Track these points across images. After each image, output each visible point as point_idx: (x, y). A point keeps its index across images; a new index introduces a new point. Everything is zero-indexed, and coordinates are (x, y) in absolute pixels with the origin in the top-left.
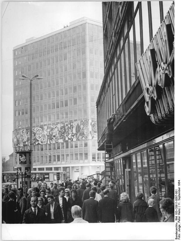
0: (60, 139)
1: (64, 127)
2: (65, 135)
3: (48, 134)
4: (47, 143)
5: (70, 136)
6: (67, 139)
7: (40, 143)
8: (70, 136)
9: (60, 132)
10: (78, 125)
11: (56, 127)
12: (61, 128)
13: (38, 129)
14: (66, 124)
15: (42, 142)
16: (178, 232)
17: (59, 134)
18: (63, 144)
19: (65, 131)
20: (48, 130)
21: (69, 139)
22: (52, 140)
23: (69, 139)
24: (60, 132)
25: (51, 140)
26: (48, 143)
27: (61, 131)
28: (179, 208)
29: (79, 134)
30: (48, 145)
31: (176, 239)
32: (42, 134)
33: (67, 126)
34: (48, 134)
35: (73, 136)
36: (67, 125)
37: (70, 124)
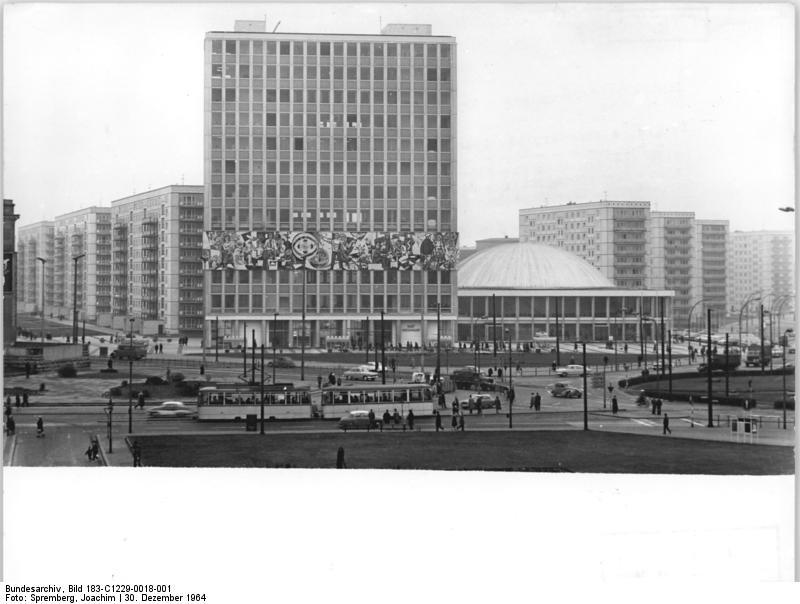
0: (373, 262)
2: (391, 256)
3: (336, 249)
4: (332, 268)
5: (403, 260)
6: (394, 264)
7: (308, 265)
8: (403, 260)
13: (301, 236)
14: (392, 234)
16: (27, 595)
17: (370, 252)
18: (378, 274)
19: (389, 246)
20: (337, 242)
21: (400, 264)
22: (348, 264)
23: (400, 264)
24: (373, 248)
25: (344, 264)
26: (337, 267)
27: (377, 247)
28: (118, 598)
29: (429, 258)
31: (8, 588)
32: (315, 247)
33: (396, 240)
34: (336, 249)
35: (414, 260)
36: (395, 237)
37: (405, 236)
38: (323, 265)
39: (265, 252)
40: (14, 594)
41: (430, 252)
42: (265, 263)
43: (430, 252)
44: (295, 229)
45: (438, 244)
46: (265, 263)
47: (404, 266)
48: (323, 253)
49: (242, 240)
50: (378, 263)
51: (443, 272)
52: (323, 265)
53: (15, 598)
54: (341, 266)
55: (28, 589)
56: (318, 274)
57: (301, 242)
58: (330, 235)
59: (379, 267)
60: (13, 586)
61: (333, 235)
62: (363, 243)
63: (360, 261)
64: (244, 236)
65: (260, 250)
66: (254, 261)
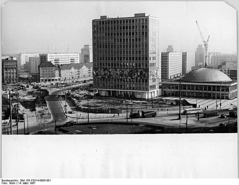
1: (132, 71)
5: (136, 76)
6: (133, 77)
7: (114, 77)
8: (136, 76)
9: (129, 73)
10: (141, 71)
11: (126, 70)
12: (130, 71)
14: (133, 70)
15: (115, 77)
16: (8, 182)
17: (128, 74)
19: (132, 73)
20: (120, 71)
24: (129, 73)
26: (120, 78)
30: (120, 79)
31: (2, 180)
33: (134, 71)
35: (138, 76)
36: (134, 70)
38: (118, 77)
39: (105, 74)
40: (4, 182)
41: (142, 74)
42: (105, 76)
43: (142, 74)
44: (111, 68)
45: (144, 72)
46: (105, 76)
47: (136, 78)
48: (117, 74)
49: (100, 70)
50: (130, 77)
51: (146, 80)
52: (118, 77)
53: (4, 183)
54: (121, 77)
55: (8, 181)
56: (117, 79)
57: (113, 71)
58: (119, 70)
59: (130, 78)
60: (4, 179)
61: (120, 70)
62: (126, 72)
63: (126, 76)
64: (100, 69)
65: (104, 73)
66: (103, 76)
